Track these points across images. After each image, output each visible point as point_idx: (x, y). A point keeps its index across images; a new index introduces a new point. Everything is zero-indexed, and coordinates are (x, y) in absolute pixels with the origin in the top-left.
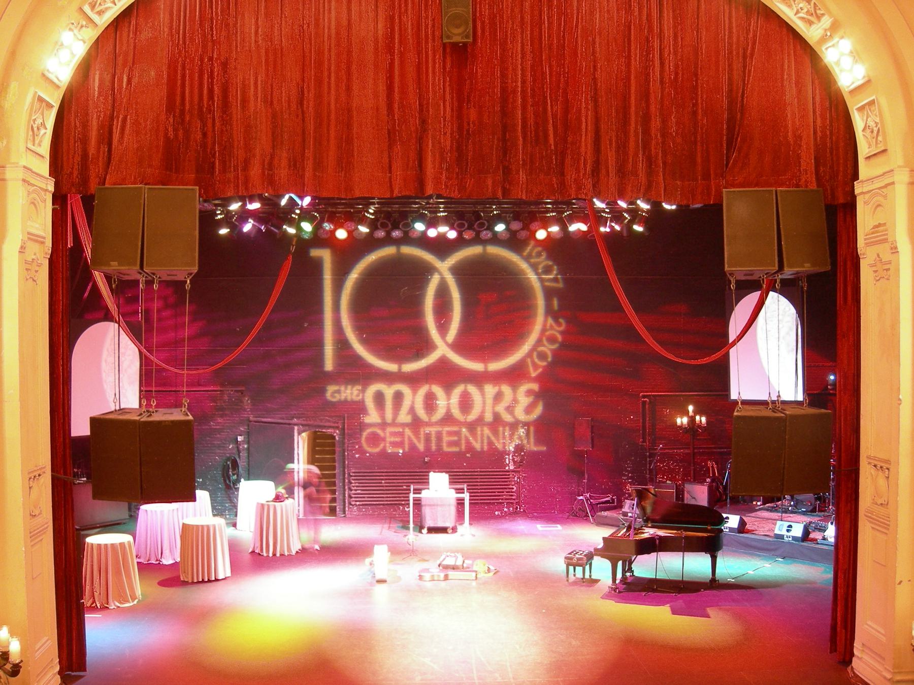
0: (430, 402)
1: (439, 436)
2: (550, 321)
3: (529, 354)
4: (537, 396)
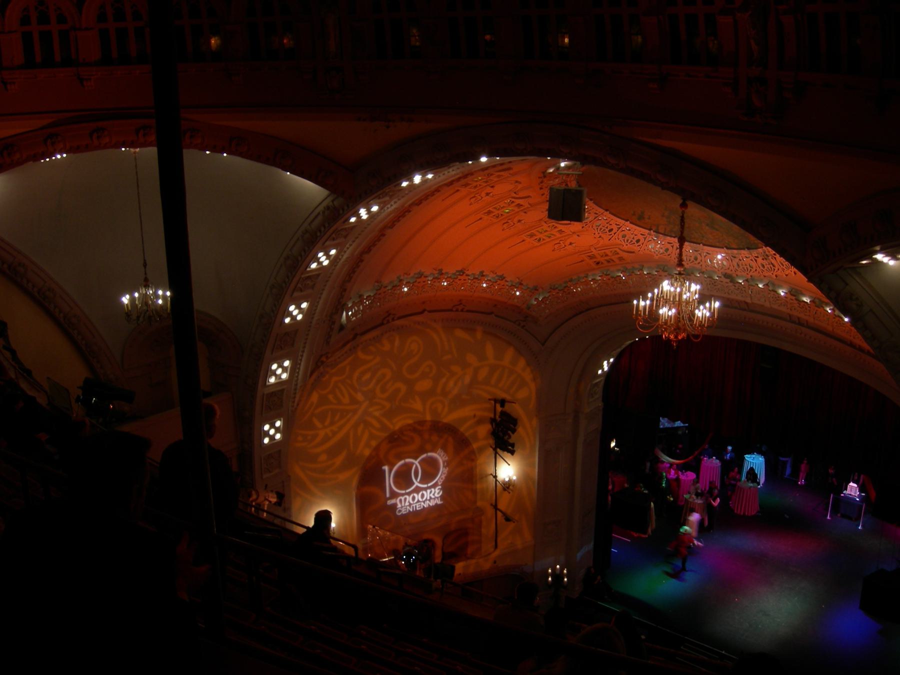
0: (414, 498)
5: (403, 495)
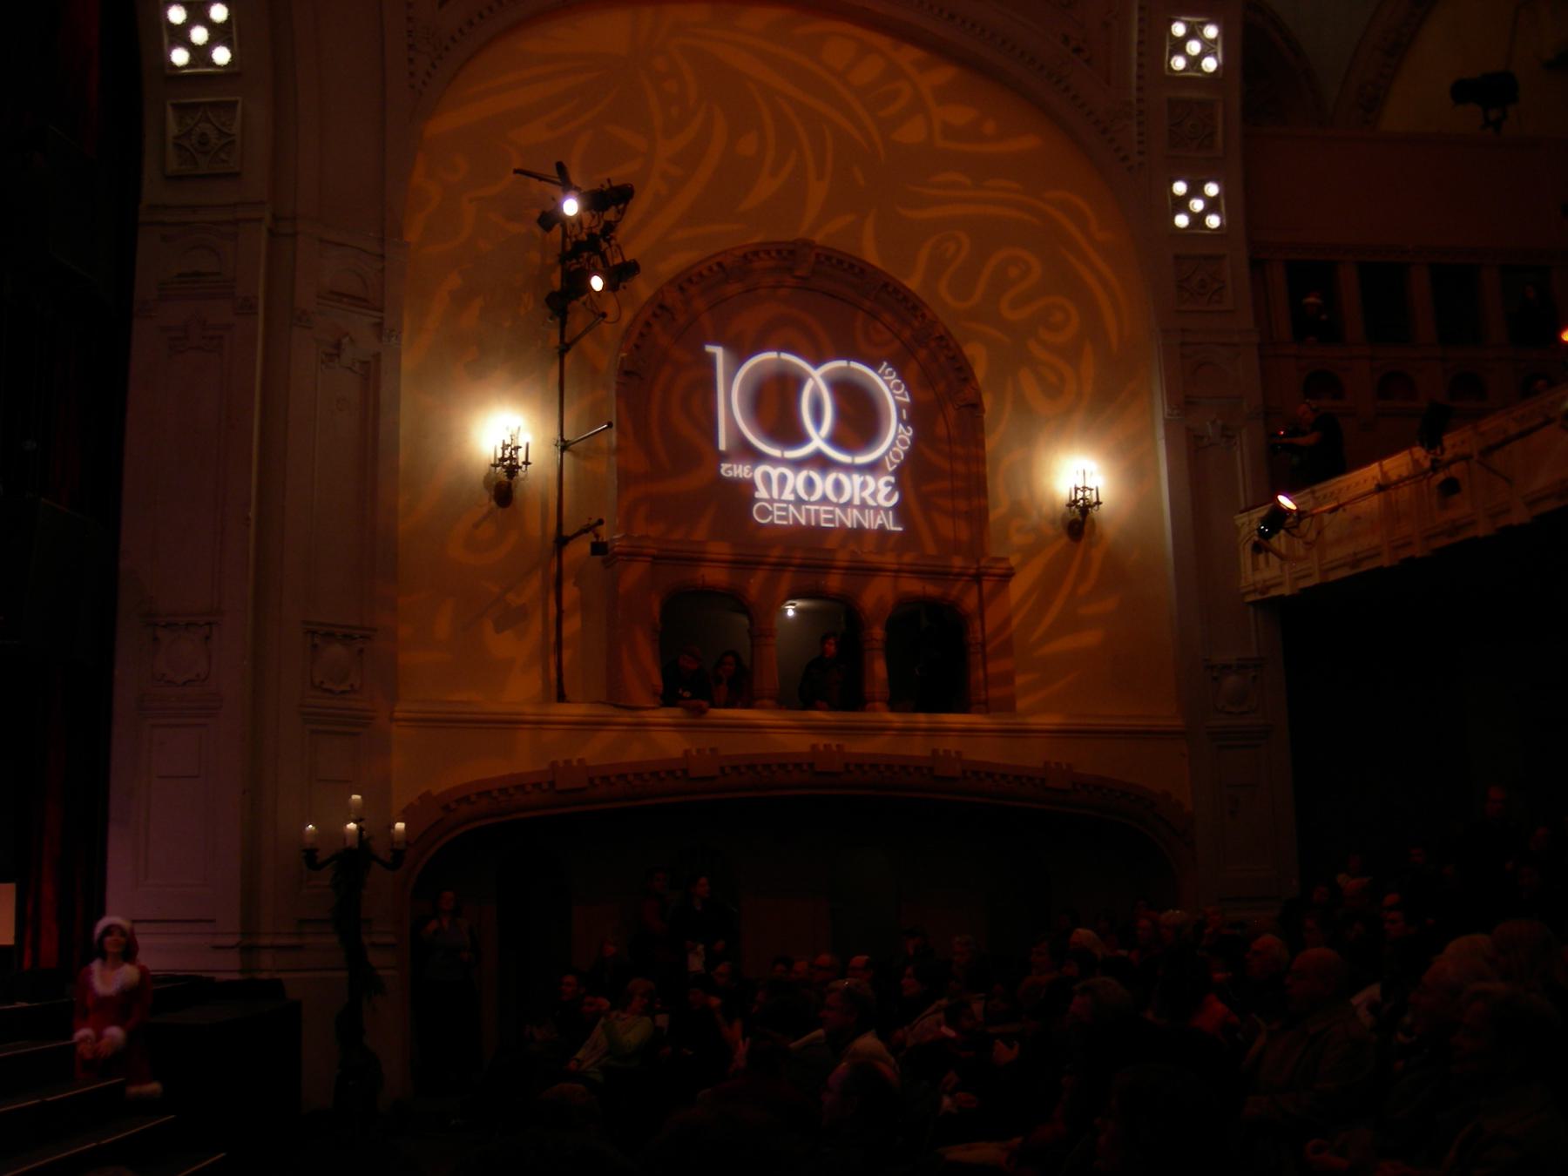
0: (810, 484)
1: (817, 512)
3: (887, 453)
5: (776, 462)
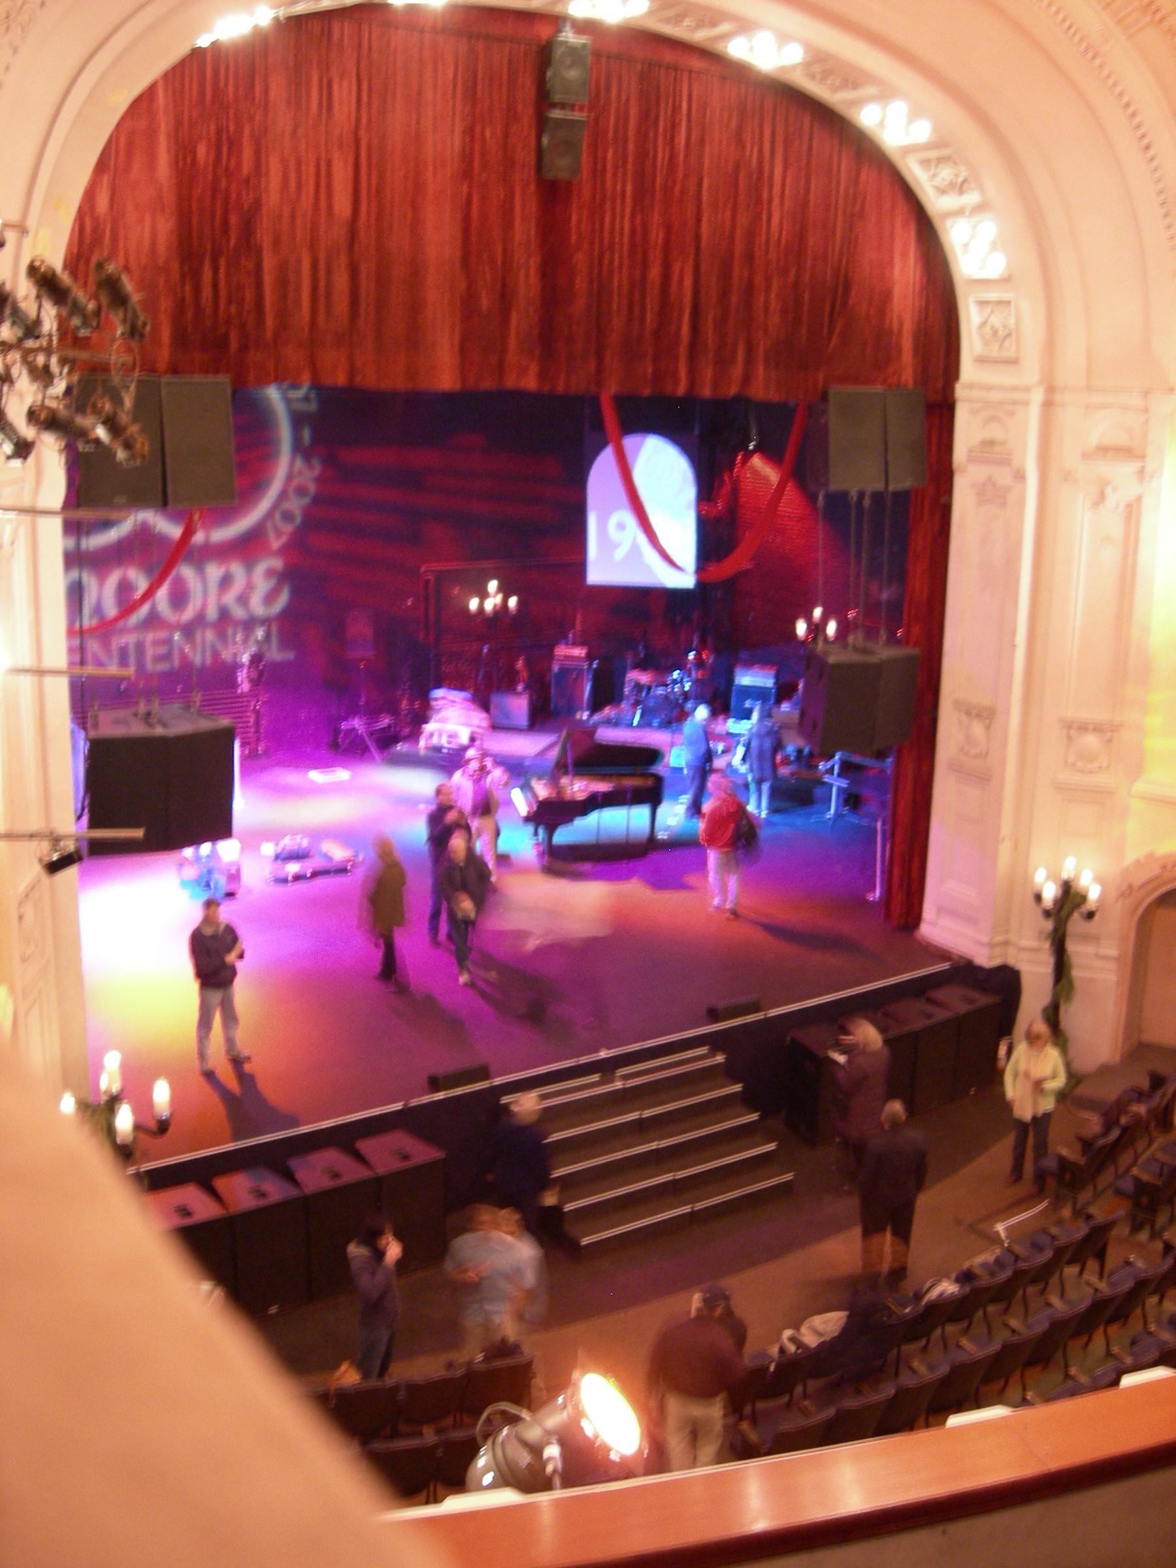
1: (140, 647)
2: (299, 463)
3: (270, 515)
4: (284, 577)
